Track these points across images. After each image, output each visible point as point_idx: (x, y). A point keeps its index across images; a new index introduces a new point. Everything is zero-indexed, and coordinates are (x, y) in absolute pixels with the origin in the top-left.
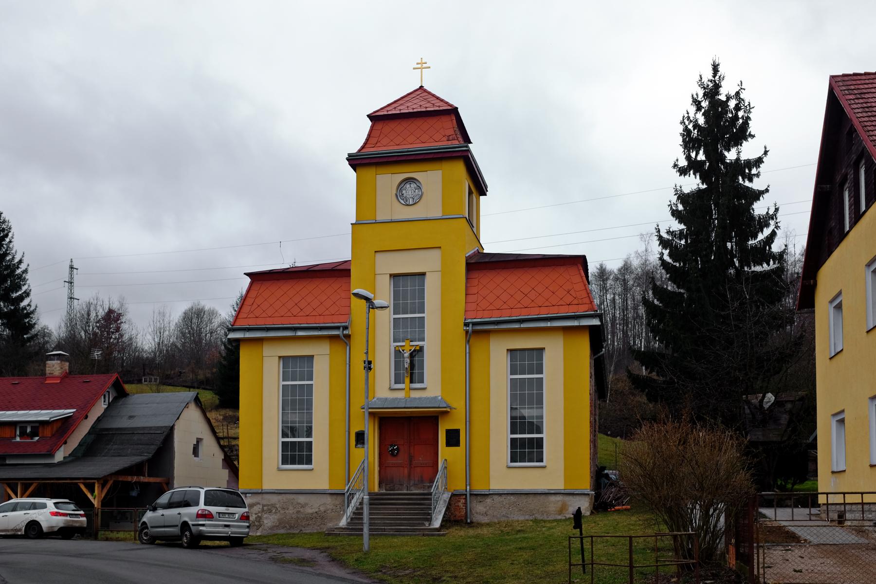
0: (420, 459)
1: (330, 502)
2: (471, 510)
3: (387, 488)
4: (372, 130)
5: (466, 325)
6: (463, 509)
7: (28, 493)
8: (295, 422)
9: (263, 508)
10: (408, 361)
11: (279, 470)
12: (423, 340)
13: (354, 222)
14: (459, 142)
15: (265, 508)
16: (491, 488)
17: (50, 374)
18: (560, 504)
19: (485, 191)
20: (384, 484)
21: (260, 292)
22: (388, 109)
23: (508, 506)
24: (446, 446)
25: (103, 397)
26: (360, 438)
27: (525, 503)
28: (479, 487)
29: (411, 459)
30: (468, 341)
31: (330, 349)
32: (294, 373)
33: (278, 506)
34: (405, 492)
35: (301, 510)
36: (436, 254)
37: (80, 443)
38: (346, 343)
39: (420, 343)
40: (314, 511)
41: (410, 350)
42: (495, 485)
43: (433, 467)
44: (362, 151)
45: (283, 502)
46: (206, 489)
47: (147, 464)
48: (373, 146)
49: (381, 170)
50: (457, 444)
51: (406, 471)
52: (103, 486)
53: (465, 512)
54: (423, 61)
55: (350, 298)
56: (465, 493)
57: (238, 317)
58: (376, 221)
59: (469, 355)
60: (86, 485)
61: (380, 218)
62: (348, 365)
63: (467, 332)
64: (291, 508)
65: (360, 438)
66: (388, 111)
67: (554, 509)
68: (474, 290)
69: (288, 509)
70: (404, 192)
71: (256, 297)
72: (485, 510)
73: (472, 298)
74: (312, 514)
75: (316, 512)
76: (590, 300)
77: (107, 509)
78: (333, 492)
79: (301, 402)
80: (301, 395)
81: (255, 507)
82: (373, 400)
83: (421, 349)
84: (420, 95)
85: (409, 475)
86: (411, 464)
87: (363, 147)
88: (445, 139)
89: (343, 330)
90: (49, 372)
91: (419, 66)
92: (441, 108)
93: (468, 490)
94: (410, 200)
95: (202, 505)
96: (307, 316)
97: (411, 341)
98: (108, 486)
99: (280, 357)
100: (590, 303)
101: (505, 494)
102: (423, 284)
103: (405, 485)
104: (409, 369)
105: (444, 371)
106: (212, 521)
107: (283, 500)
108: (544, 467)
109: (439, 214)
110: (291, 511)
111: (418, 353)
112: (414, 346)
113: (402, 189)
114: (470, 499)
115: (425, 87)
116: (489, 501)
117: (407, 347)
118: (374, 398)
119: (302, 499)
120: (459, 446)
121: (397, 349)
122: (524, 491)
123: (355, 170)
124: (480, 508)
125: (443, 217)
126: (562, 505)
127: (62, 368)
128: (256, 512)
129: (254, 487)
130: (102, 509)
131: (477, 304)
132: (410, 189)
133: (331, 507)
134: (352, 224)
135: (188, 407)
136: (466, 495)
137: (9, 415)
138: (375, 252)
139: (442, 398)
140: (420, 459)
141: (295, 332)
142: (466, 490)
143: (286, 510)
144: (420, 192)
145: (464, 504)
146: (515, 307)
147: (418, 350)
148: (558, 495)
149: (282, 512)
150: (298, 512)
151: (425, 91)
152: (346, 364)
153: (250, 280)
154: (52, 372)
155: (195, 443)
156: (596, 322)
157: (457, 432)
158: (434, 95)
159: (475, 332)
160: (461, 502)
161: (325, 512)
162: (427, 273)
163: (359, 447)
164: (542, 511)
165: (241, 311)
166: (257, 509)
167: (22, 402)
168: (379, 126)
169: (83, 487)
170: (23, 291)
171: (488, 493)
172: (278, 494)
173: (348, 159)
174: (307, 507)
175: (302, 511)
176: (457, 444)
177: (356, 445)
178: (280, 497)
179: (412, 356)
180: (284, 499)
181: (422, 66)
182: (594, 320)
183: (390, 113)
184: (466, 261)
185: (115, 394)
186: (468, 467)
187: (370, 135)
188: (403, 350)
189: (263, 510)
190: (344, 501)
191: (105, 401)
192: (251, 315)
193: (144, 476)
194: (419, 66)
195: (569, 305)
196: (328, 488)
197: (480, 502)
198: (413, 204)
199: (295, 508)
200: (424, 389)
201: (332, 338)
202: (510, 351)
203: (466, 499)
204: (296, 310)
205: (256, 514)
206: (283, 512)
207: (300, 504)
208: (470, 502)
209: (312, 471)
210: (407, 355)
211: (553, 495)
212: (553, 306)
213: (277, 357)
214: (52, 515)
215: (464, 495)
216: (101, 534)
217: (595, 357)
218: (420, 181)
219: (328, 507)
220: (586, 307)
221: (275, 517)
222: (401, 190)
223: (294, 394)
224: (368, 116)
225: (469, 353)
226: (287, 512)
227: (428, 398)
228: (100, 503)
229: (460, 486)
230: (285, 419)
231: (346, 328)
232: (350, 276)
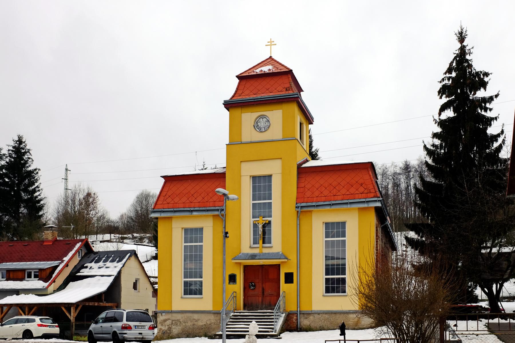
0: (269, 291)
2: (300, 323)
3: (249, 309)
4: (239, 85)
7: (31, 313)
9: (172, 322)
10: (262, 230)
12: (271, 216)
13: (228, 143)
14: (293, 91)
15: (174, 322)
16: (312, 310)
17: (46, 239)
19: (312, 121)
20: (246, 307)
21: (171, 187)
22: (249, 71)
23: (323, 321)
24: (285, 283)
25: (78, 253)
26: (232, 278)
27: (334, 319)
28: (304, 308)
30: (298, 216)
31: (213, 223)
32: (191, 238)
33: (181, 321)
35: (196, 323)
36: (279, 163)
37: (64, 282)
39: (269, 219)
40: (204, 323)
41: (263, 223)
42: (316, 307)
43: (277, 296)
44: (233, 99)
46: (127, 311)
47: (104, 295)
49: (244, 110)
51: (260, 299)
52: (76, 309)
53: (296, 324)
54: (272, 41)
56: (297, 313)
59: (299, 226)
60: (65, 308)
61: (244, 140)
63: (298, 212)
65: (232, 278)
68: (302, 185)
69: (187, 323)
70: (259, 124)
71: (168, 191)
72: (309, 323)
74: (202, 326)
75: (205, 325)
76: (375, 191)
77: (78, 323)
79: (196, 256)
80: (196, 251)
81: (167, 321)
82: (240, 255)
83: (270, 222)
84: (270, 62)
85: (262, 301)
87: (233, 96)
88: (284, 90)
89: (221, 211)
90: (46, 238)
91: (269, 44)
92: (282, 71)
93: (298, 311)
94: (263, 129)
95: (125, 321)
96: (199, 202)
97: (263, 218)
98: (79, 308)
99: (182, 228)
100: (374, 192)
101: (321, 313)
102: (270, 181)
103: (259, 308)
104: (262, 235)
105: (283, 235)
106: (131, 331)
107: (184, 317)
110: (189, 324)
111: (267, 225)
112: (265, 220)
115: (273, 57)
116: (311, 317)
117: (261, 221)
118: (240, 253)
119: (196, 316)
121: (254, 222)
122: (334, 311)
123: (228, 111)
124: (306, 322)
125: (283, 139)
127: (53, 236)
128: (168, 325)
129: (167, 308)
130: (75, 323)
131: (304, 194)
134: (226, 145)
135: (130, 259)
136: (297, 314)
137: (22, 264)
138: (241, 162)
139: (282, 253)
140: (269, 291)
142: (297, 311)
143: (186, 323)
145: (296, 319)
146: (328, 195)
147: (268, 223)
149: (184, 324)
150: (194, 325)
151: (273, 59)
154: (47, 238)
155: (135, 282)
156: (379, 204)
158: (278, 62)
162: (273, 175)
163: (231, 284)
165: (159, 200)
166: (168, 322)
167: (29, 256)
169: (64, 309)
170: (35, 186)
171: (311, 313)
172: (182, 314)
173: (223, 104)
177: (229, 283)
178: (183, 315)
179: (264, 226)
181: (271, 43)
182: (377, 203)
183: (250, 74)
184: (297, 167)
185: (86, 251)
186: (298, 296)
187: (237, 89)
188: (258, 223)
189: (172, 324)
191: (79, 256)
192: (165, 202)
193: (102, 302)
194: (269, 44)
195: (362, 194)
196: (212, 310)
197: (306, 318)
199: (192, 322)
200: (271, 247)
203: (297, 316)
205: (168, 326)
206: (185, 324)
207: (195, 319)
208: (300, 318)
209: (202, 299)
210: (260, 226)
211: (352, 314)
214: (38, 326)
216: (74, 337)
217: (382, 226)
218: (267, 115)
219: (212, 321)
220: (372, 195)
221: (180, 328)
222: (257, 123)
223: (191, 251)
224: (237, 76)
225: (299, 225)
227: (274, 253)
228: (74, 319)
229: (293, 308)
230: (186, 267)
232: (225, 178)
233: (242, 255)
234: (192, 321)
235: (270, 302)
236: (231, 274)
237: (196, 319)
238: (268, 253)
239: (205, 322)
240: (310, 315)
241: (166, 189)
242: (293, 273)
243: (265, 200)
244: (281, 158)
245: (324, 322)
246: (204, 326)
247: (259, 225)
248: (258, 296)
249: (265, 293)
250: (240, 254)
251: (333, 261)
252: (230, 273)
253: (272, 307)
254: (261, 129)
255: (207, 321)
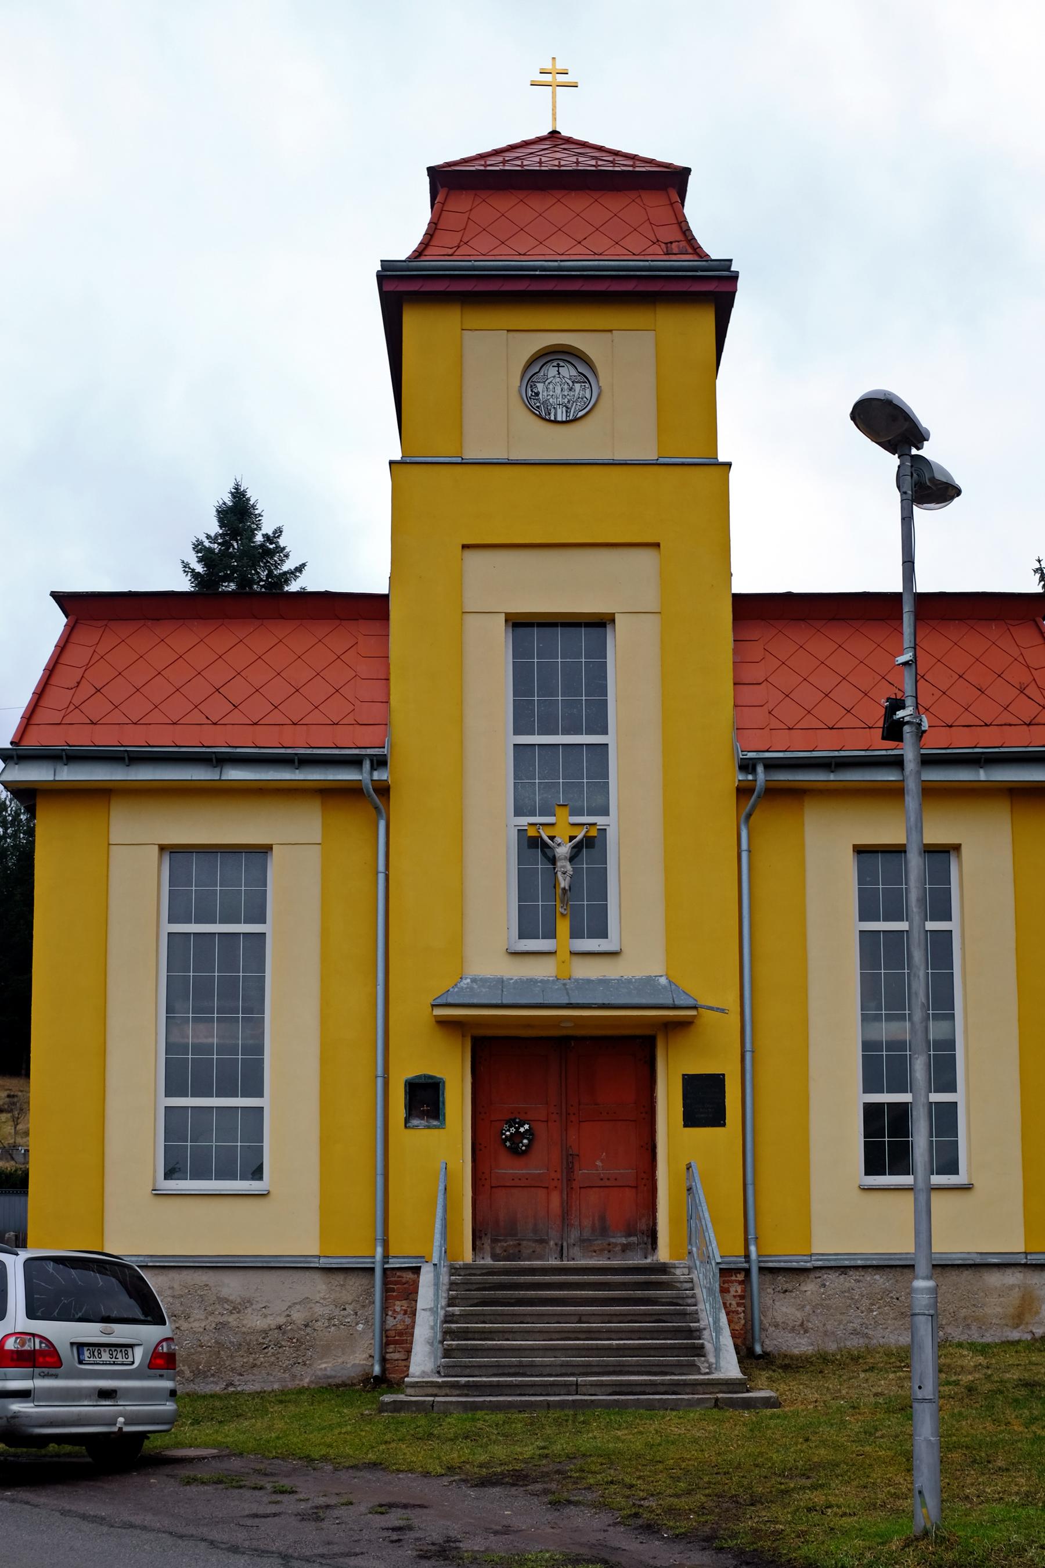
0: (599, 1163)
1: (322, 1295)
3: (498, 1251)
5: (747, 766)
6: (737, 1313)
8: (207, 1049)
11: (159, 1194)
13: (397, 456)
18: (1016, 1294)
20: (487, 1242)
21: (101, 650)
23: (866, 1302)
24: (685, 1126)
29: (570, 1162)
34: (554, 1262)
35: (231, 1319)
38: (376, 808)
39: (600, 820)
40: (271, 1322)
41: (572, 838)
43: (636, 1187)
45: (173, 1297)
48: (451, 251)
50: (717, 1119)
53: (743, 1322)
55: (388, 679)
56: (746, 1265)
57: (33, 722)
58: (462, 459)
62: (381, 877)
64: (198, 1313)
66: (486, 165)
67: (999, 1309)
68: (756, 673)
69: (187, 1317)
70: (540, 387)
72: (799, 1315)
73: (750, 694)
74: (265, 1332)
75: (279, 1328)
78: (334, 1263)
80: (229, 963)
86: (569, 1180)
93: (754, 1256)
94: (559, 411)
96: (255, 724)
99: (162, 848)
101: (856, 1267)
103: (552, 1243)
108: (967, 1188)
109: (651, 455)
110: (196, 1324)
112: (584, 824)
113: (534, 379)
114: (760, 1284)
116: (810, 1287)
119: (232, 1286)
120: (724, 1125)
124: (784, 1309)
125: (661, 461)
126: (1023, 1298)
132: (558, 380)
133: (326, 1311)
136: (747, 1272)
138: (465, 547)
140: (599, 1163)
141: (218, 770)
142: (747, 1256)
144: (588, 391)
145: (742, 1297)
148: (1009, 1271)
150: (221, 1327)
152: (377, 873)
153: (64, 620)
157: (717, 1082)
159: (773, 793)
160: (733, 1293)
161: (306, 1326)
164: (965, 1318)
168: (461, 203)
171: (809, 1265)
172: (156, 1271)
174: (249, 1310)
175: (234, 1324)
176: (717, 1119)
177: (407, 1121)
180: (176, 1286)
187: (436, 224)
190: (369, 1293)
192: (75, 717)
195: (1029, 725)
197: (786, 1291)
198: (562, 422)
201: (328, 793)
202: (860, 851)
204: (217, 708)
207: (227, 1301)
211: (995, 1270)
212: (986, 725)
213: (157, 846)
215: (738, 1271)
219: (319, 1310)
222: (531, 383)
226: (185, 1325)
231: (380, 762)
233: (475, 986)
234: (210, 1309)
235: (603, 1219)
236: (419, 1077)
237: (231, 1298)
238: (604, 982)
239: (280, 1315)
240: (802, 1279)
241: (77, 655)
242: (724, 1075)
243: (578, 732)
244: (657, 545)
245: (872, 1311)
246: (276, 1334)
247: (559, 845)
248: (547, 1188)
249: (581, 1173)
250: (465, 982)
251: (895, 1025)
252: (411, 1073)
253: (613, 1240)
254: (553, 411)
255: (290, 1307)
